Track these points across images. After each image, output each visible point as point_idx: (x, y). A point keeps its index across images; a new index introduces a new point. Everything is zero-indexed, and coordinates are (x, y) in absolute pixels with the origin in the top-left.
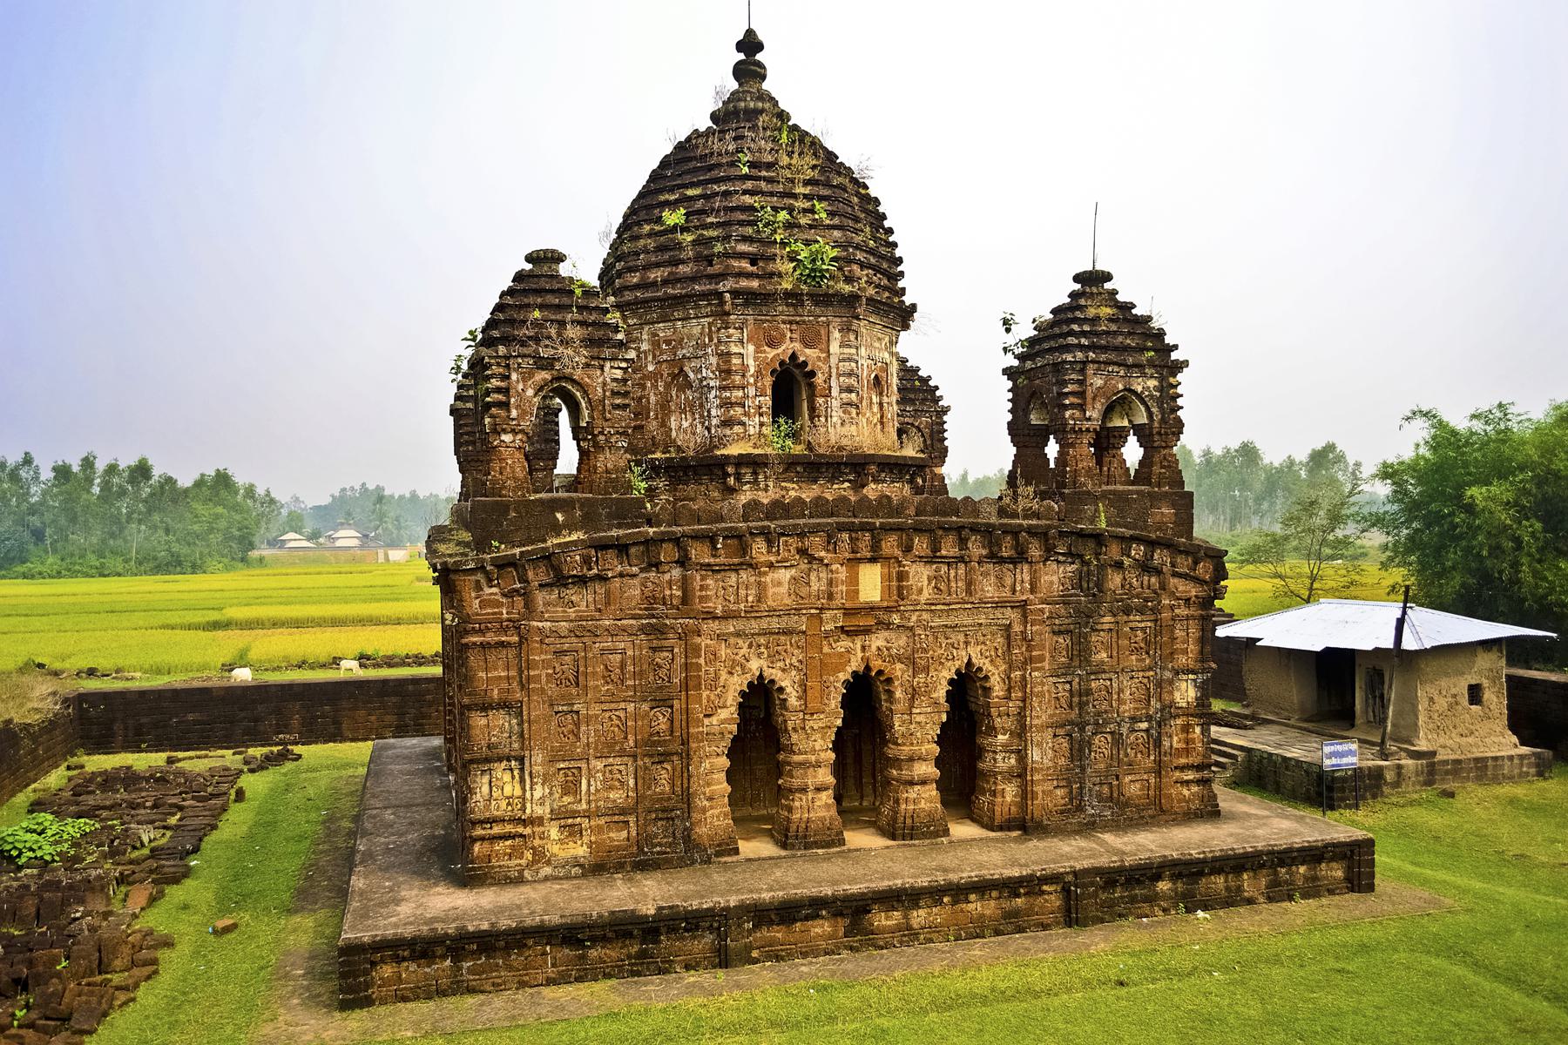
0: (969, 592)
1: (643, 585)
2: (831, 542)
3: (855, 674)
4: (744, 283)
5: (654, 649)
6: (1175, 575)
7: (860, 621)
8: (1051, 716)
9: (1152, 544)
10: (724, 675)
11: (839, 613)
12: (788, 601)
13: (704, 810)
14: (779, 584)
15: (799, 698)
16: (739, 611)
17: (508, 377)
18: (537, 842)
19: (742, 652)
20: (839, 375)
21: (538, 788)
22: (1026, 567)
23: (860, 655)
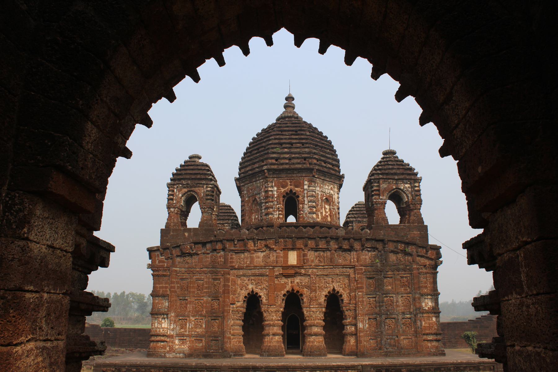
0: (331, 262)
1: (211, 257)
2: (276, 243)
3: (288, 292)
4: (273, 167)
5: (214, 279)
6: (418, 256)
7: (291, 272)
8: (367, 311)
9: (408, 244)
10: (239, 290)
11: (281, 269)
12: (262, 264)
13: (229, 338)
14: (259, 257)
15: (266, 300)
17: (173, 191)
18: (171, 344)
19: (245, 282)
20: (307, 197)
21: (172, 325)
22: (355, 253)
23: (290, 285)
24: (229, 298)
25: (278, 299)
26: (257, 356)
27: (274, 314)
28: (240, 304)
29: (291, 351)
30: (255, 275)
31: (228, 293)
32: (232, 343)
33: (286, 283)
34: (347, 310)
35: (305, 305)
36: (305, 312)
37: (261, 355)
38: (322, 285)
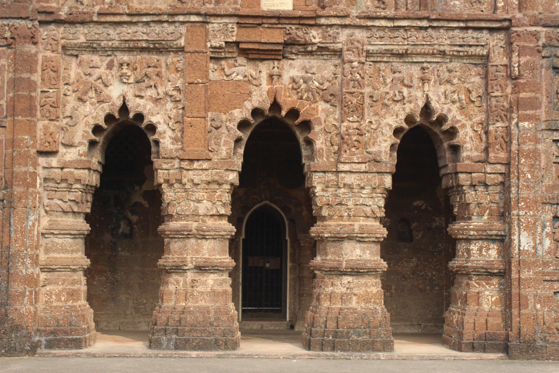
3: (256, 112)
10: (72, 101)
11: (231, 23)
13: (31, 281)
15: (175, 140)
16: (91, 14)
19: (97, 73)
23: (265, 87)
24: (31, 130)
25: (218, 138)
26: (138, 346)
27: (200, 194)
28: (78, 158)
29: (255, 325)
30: (132, 48)
31: (31, 111)
32: (43, 298)
33: (249, 80)
34: (473, 186)
35: (321, 161)
36: (318, 190)
37: (153, 344)
38: (383, 89)
